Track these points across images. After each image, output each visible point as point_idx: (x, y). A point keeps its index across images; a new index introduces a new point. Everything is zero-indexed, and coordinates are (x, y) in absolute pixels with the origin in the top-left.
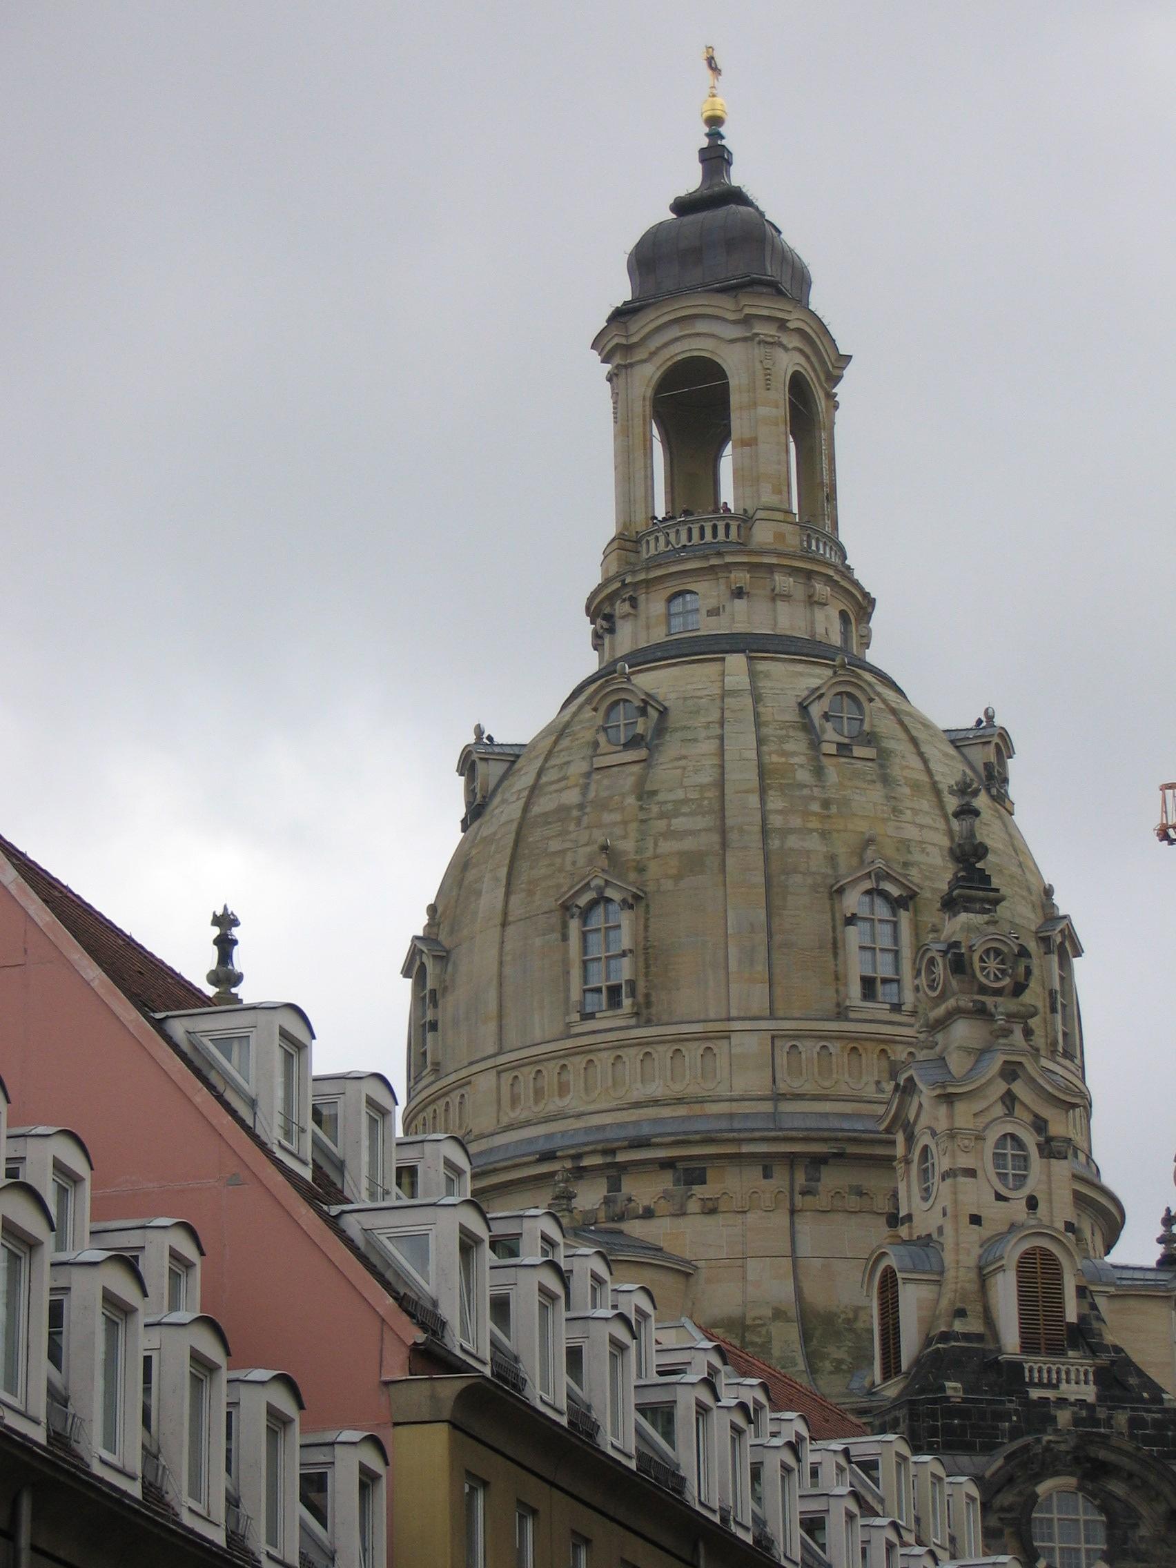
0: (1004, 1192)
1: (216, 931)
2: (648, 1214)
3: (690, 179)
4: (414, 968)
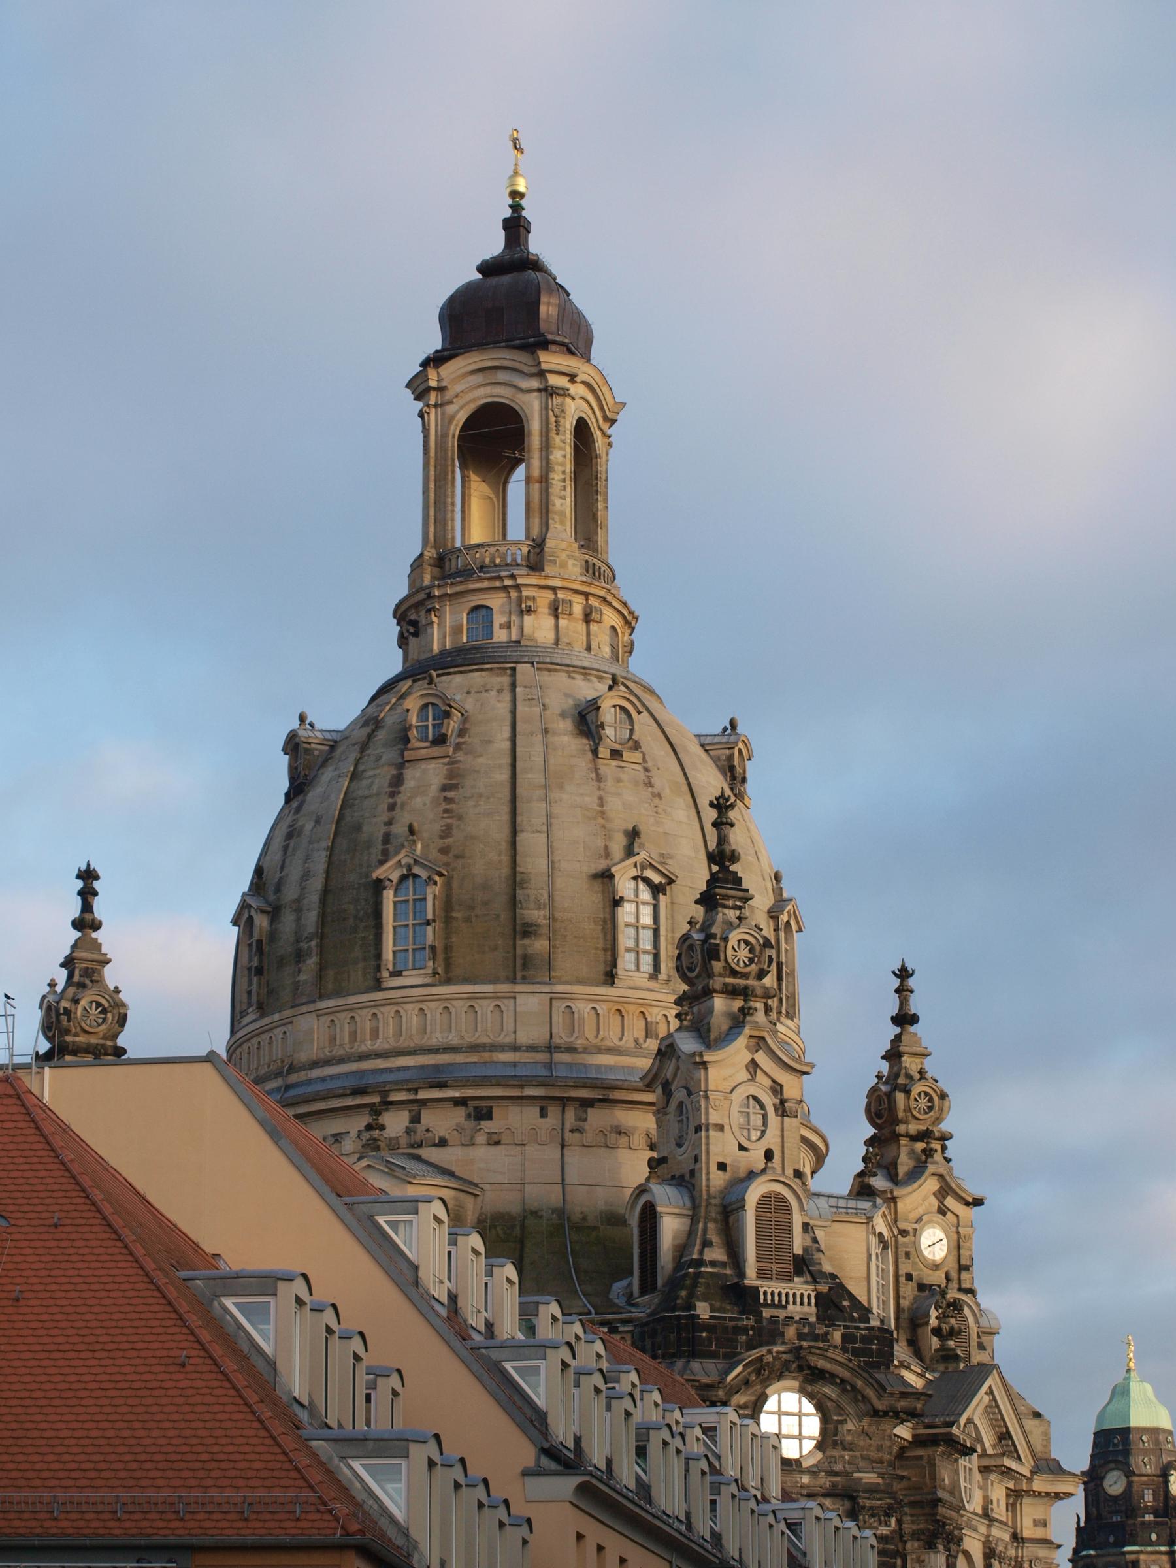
0: (745, 1144)
1: (80, 884)
2: (443, 1143)
3: (494, 245)
4: (243, 918)
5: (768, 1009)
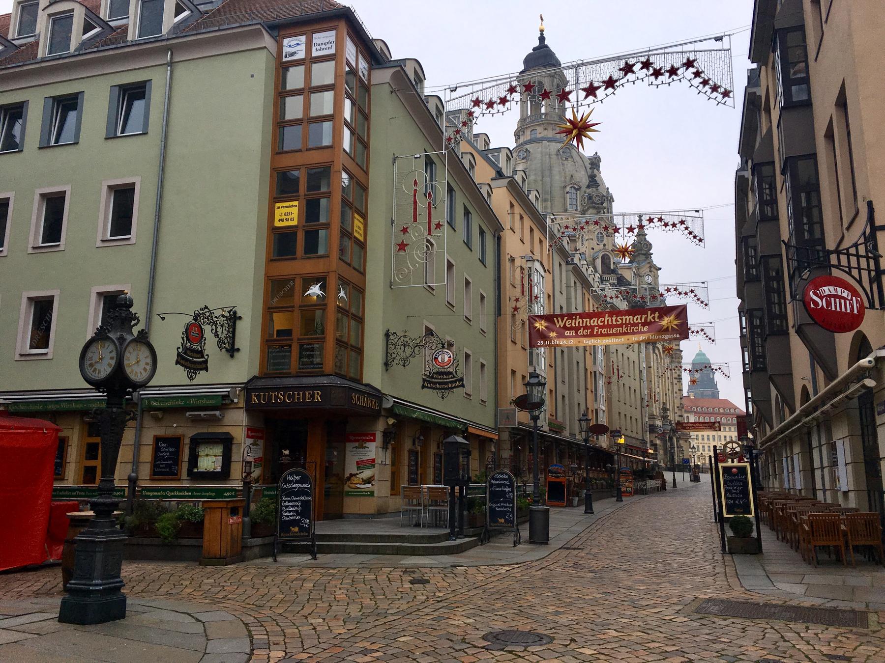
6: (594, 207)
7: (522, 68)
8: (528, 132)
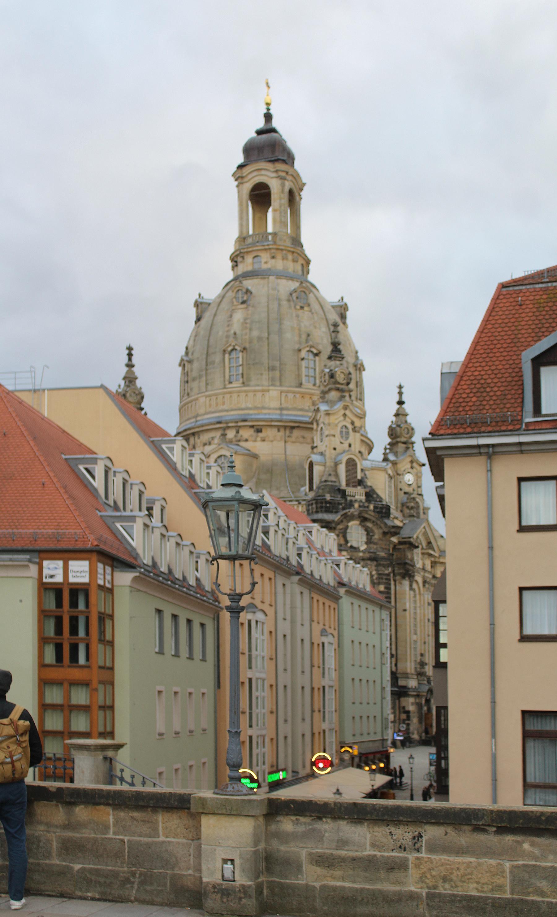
0: (342, 441)
5: (350, 396)
6: (338, 389)
7: (240, 159)
8: (249, 259)
